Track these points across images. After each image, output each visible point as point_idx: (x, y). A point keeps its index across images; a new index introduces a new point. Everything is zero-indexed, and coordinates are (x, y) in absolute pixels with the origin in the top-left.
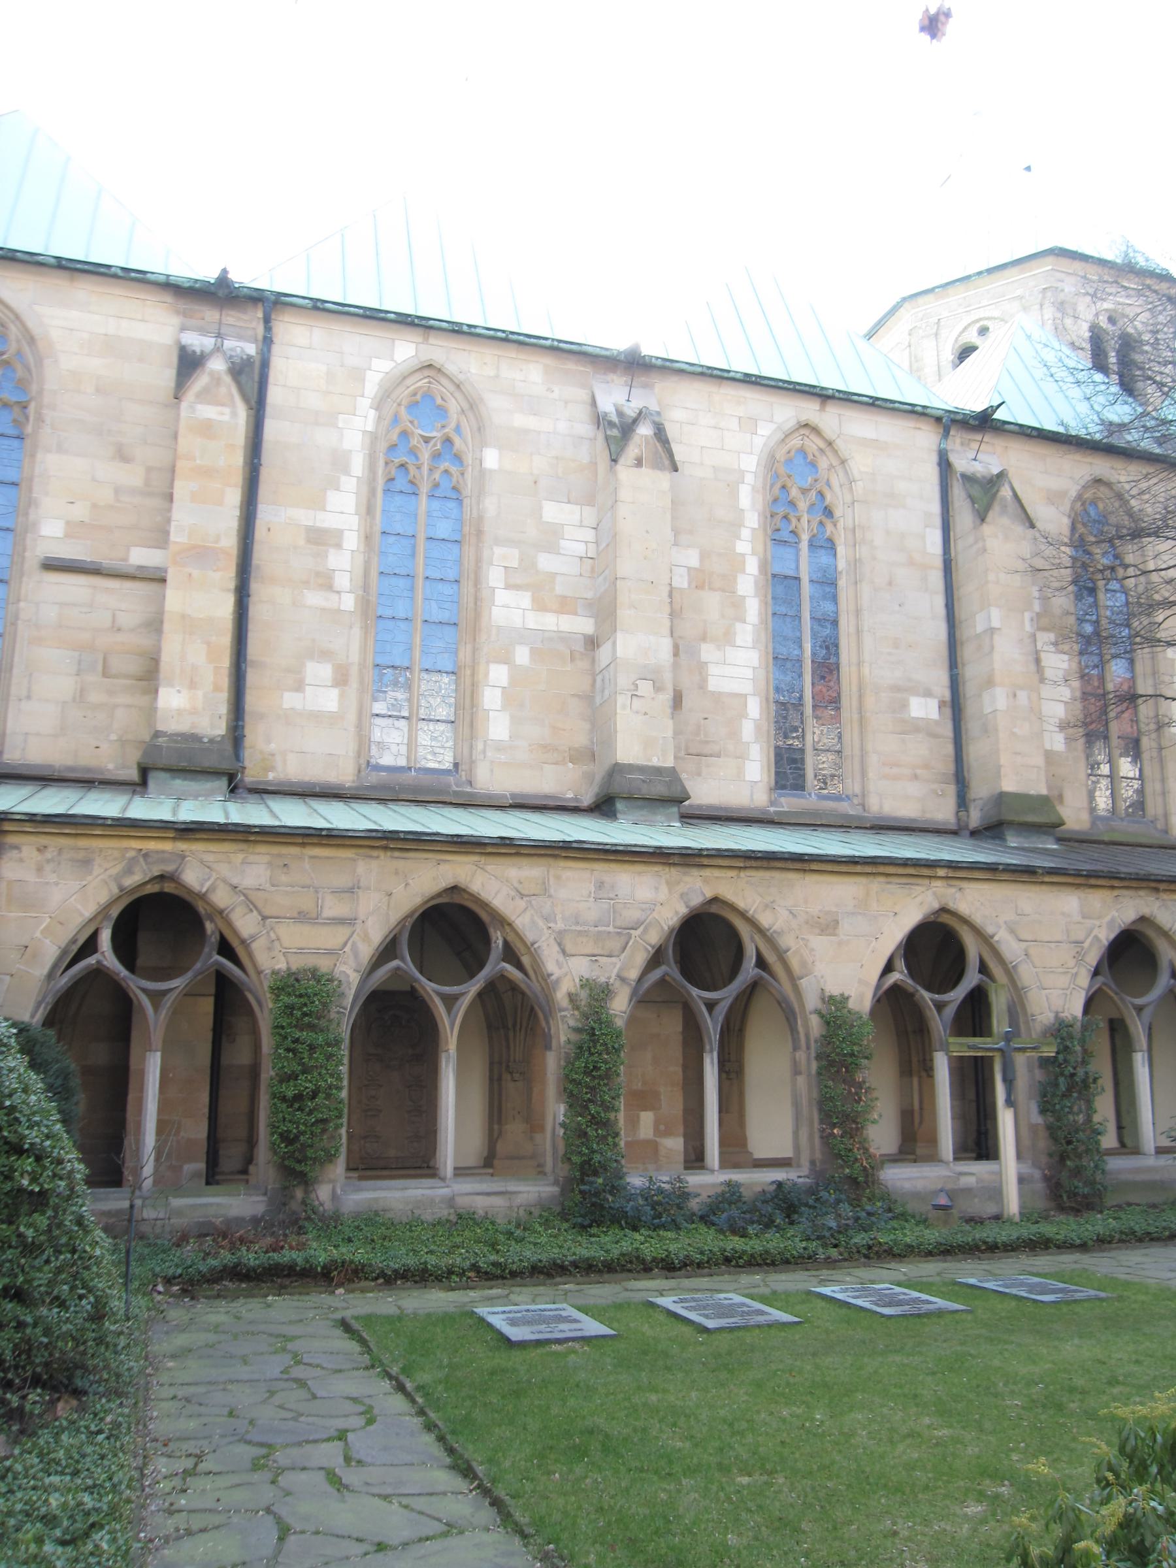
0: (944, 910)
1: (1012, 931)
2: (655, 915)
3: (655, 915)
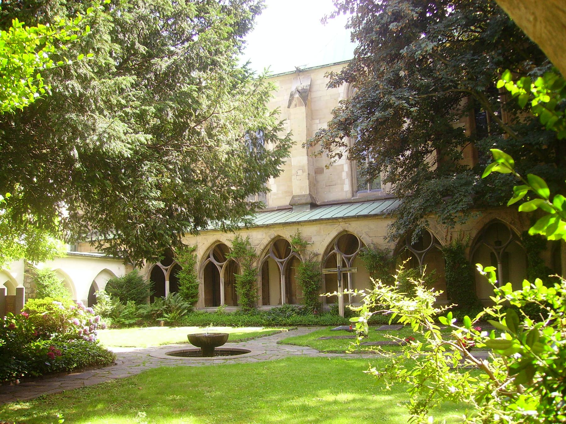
0: (345, 231)
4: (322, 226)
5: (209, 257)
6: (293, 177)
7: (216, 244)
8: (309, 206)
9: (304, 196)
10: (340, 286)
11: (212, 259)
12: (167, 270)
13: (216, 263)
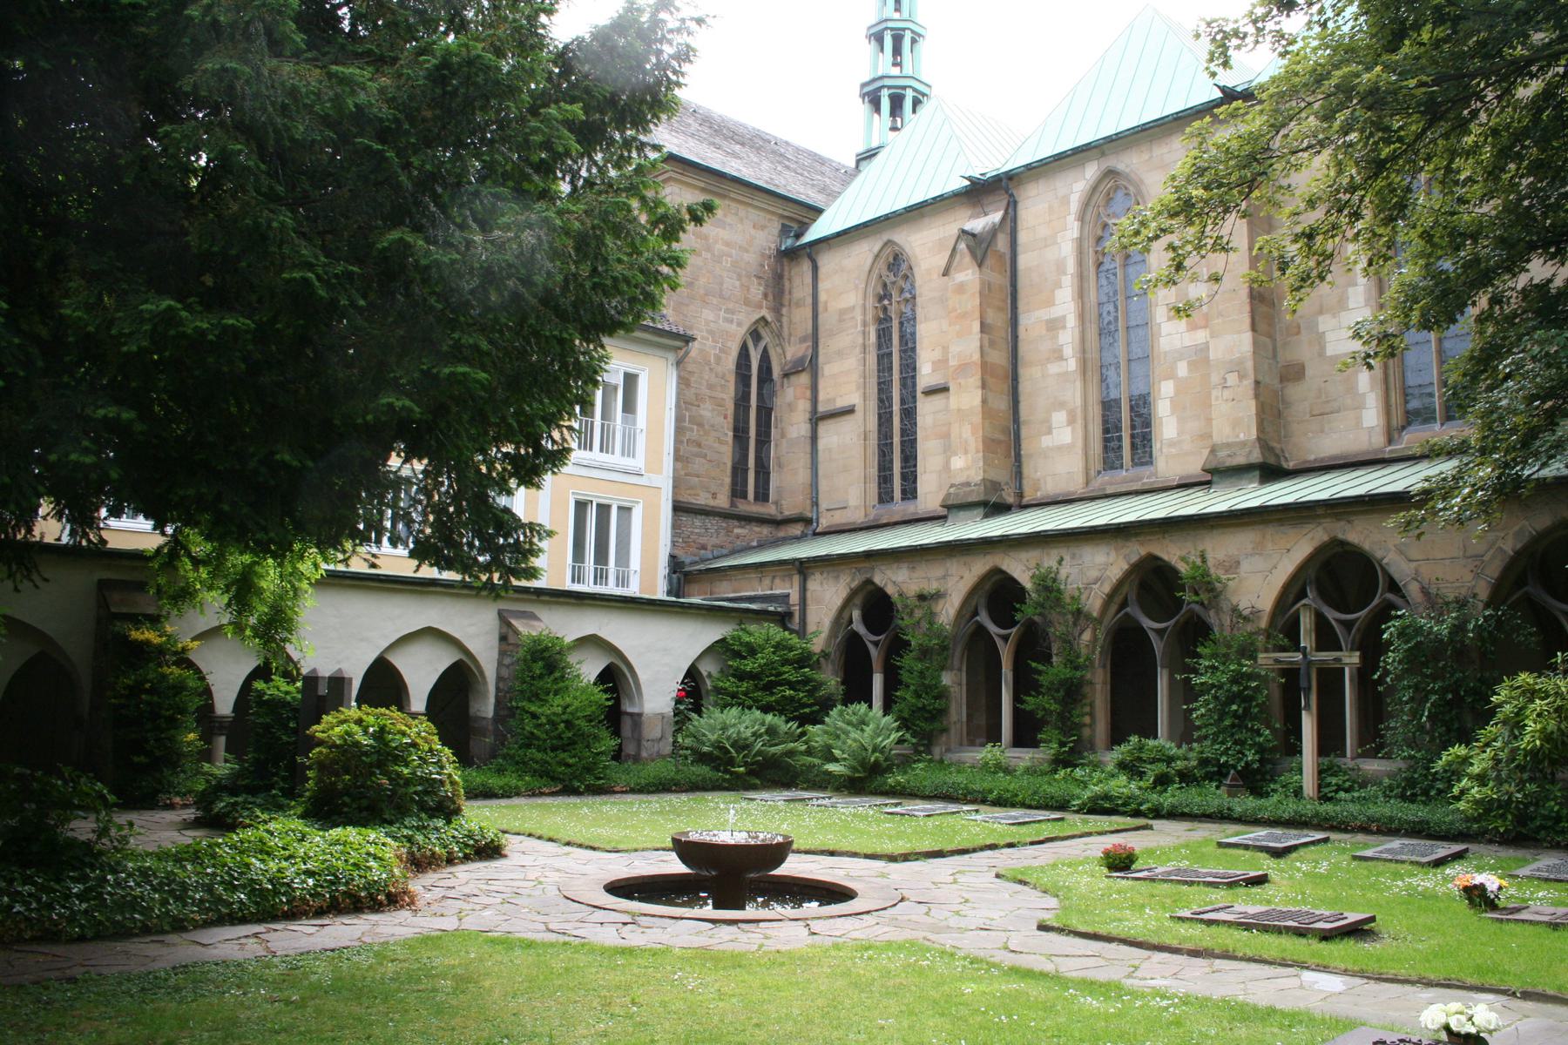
1: (1401, 553)
2: (1108, 573)
3: (1108, 573)
4: (1270, 531)
5: (976, 613)
6: (1214, 393)
7: (994, 579)
8: (1257, 473)
9: (1243, 444)
10: (1308, 707)
11: (984, 618)
12: (876, 644)
13: (993, 629)
